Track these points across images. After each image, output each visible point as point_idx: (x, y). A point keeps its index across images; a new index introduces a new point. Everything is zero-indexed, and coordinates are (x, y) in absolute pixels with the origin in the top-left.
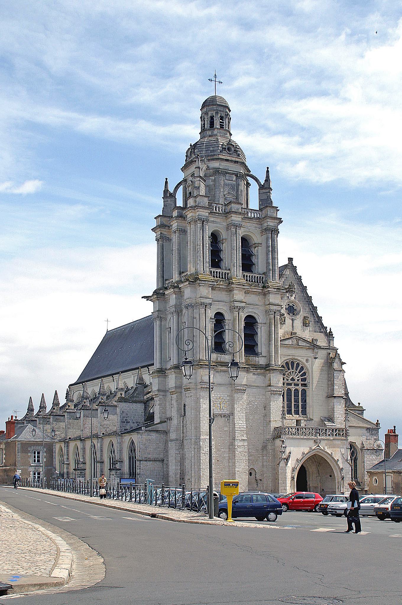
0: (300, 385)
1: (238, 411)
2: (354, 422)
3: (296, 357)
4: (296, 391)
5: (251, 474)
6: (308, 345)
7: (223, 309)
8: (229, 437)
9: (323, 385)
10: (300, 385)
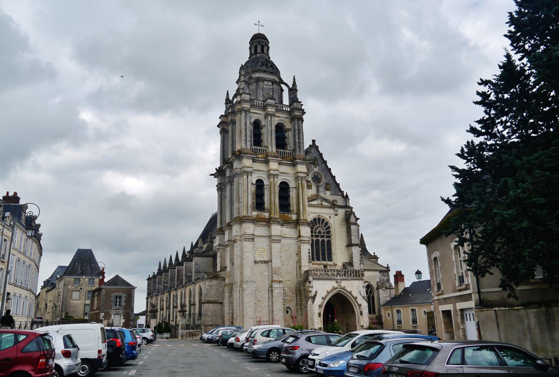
0: (325, 237)
2: (368, 264)
3: (321, 215)
4: (323, 241)
5: (287, 312)
6: (330, 205)
7: (263, 177)
8: (269, 280)
9: (343, 237)
10: (325, 237)
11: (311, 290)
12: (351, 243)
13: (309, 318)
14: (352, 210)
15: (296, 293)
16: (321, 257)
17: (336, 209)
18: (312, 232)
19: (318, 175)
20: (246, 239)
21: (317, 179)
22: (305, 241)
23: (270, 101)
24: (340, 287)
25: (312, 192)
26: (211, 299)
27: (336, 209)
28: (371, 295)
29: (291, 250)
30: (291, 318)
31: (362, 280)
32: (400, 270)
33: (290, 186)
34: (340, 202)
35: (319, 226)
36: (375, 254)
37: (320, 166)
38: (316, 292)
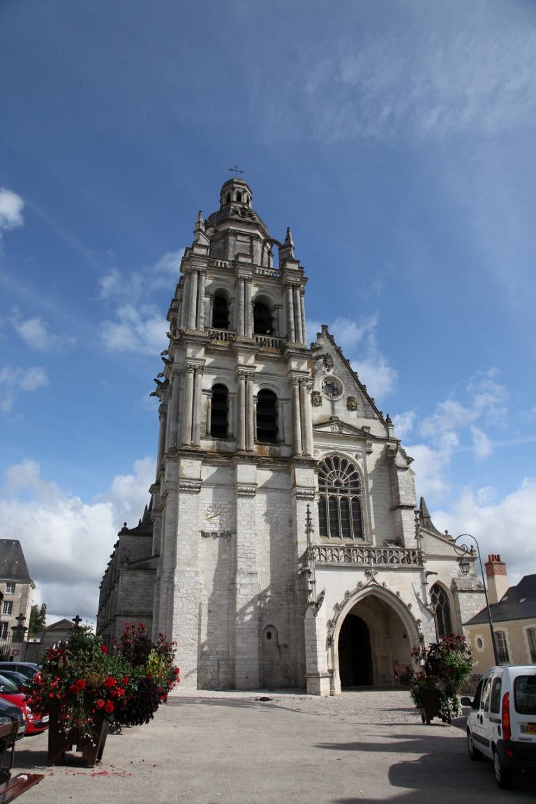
1: (244, 526)
4: (343, 499)
5: (269, 636)
6: (355, 434)
8: (230, 570)
9: (383, 492)
11: (310, 588)
12: (399, 502)
13: (306, 648)
14: (398, 444)
15: (288, 596)
16: (341, 530)
17: (368, 441)
18: (321, 482)
19: (333, 384)
20: (185, 487)
21: (332, 388)
22: (305, 494)
23: (242, 259)
24: (373, 583)
25: (324, 410)
26: (132, 609)
27: (368, 441)
28: (444, 605)
29: (279, 513)
30: (275, 648)
31: (421, 569)
32: (496, 554)
33: (279, 396)
34: (376, 429)
35: (337, 472)
36: (449, 534)
37: (337, 368)
38: (323, 593)
